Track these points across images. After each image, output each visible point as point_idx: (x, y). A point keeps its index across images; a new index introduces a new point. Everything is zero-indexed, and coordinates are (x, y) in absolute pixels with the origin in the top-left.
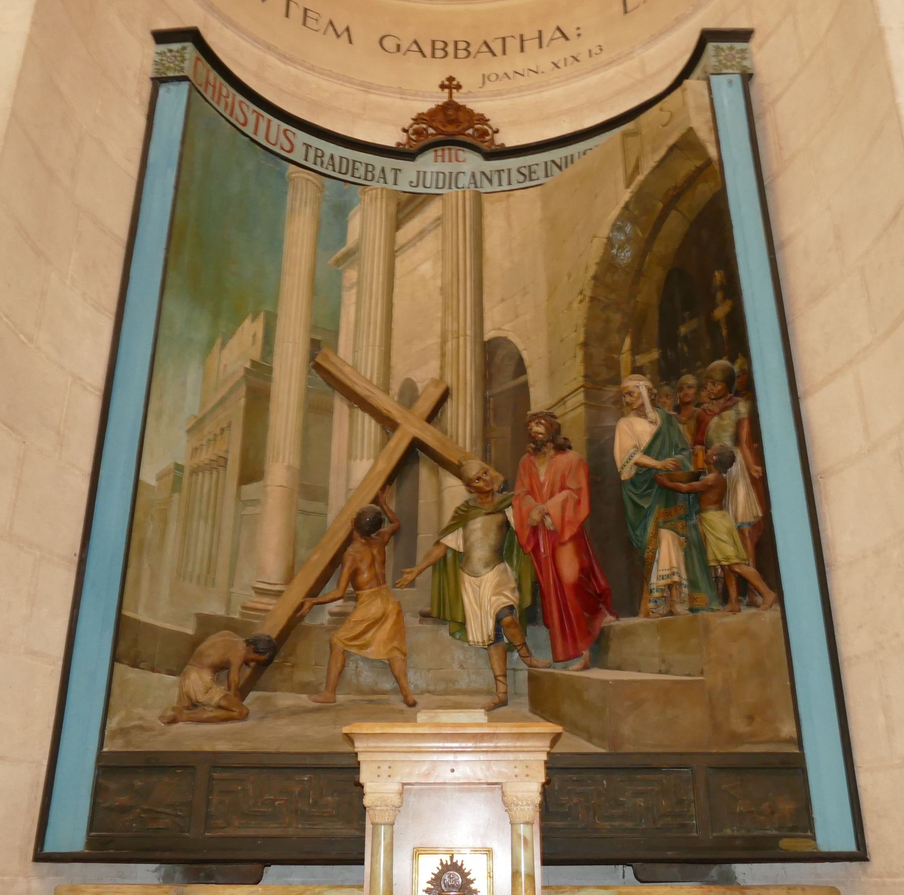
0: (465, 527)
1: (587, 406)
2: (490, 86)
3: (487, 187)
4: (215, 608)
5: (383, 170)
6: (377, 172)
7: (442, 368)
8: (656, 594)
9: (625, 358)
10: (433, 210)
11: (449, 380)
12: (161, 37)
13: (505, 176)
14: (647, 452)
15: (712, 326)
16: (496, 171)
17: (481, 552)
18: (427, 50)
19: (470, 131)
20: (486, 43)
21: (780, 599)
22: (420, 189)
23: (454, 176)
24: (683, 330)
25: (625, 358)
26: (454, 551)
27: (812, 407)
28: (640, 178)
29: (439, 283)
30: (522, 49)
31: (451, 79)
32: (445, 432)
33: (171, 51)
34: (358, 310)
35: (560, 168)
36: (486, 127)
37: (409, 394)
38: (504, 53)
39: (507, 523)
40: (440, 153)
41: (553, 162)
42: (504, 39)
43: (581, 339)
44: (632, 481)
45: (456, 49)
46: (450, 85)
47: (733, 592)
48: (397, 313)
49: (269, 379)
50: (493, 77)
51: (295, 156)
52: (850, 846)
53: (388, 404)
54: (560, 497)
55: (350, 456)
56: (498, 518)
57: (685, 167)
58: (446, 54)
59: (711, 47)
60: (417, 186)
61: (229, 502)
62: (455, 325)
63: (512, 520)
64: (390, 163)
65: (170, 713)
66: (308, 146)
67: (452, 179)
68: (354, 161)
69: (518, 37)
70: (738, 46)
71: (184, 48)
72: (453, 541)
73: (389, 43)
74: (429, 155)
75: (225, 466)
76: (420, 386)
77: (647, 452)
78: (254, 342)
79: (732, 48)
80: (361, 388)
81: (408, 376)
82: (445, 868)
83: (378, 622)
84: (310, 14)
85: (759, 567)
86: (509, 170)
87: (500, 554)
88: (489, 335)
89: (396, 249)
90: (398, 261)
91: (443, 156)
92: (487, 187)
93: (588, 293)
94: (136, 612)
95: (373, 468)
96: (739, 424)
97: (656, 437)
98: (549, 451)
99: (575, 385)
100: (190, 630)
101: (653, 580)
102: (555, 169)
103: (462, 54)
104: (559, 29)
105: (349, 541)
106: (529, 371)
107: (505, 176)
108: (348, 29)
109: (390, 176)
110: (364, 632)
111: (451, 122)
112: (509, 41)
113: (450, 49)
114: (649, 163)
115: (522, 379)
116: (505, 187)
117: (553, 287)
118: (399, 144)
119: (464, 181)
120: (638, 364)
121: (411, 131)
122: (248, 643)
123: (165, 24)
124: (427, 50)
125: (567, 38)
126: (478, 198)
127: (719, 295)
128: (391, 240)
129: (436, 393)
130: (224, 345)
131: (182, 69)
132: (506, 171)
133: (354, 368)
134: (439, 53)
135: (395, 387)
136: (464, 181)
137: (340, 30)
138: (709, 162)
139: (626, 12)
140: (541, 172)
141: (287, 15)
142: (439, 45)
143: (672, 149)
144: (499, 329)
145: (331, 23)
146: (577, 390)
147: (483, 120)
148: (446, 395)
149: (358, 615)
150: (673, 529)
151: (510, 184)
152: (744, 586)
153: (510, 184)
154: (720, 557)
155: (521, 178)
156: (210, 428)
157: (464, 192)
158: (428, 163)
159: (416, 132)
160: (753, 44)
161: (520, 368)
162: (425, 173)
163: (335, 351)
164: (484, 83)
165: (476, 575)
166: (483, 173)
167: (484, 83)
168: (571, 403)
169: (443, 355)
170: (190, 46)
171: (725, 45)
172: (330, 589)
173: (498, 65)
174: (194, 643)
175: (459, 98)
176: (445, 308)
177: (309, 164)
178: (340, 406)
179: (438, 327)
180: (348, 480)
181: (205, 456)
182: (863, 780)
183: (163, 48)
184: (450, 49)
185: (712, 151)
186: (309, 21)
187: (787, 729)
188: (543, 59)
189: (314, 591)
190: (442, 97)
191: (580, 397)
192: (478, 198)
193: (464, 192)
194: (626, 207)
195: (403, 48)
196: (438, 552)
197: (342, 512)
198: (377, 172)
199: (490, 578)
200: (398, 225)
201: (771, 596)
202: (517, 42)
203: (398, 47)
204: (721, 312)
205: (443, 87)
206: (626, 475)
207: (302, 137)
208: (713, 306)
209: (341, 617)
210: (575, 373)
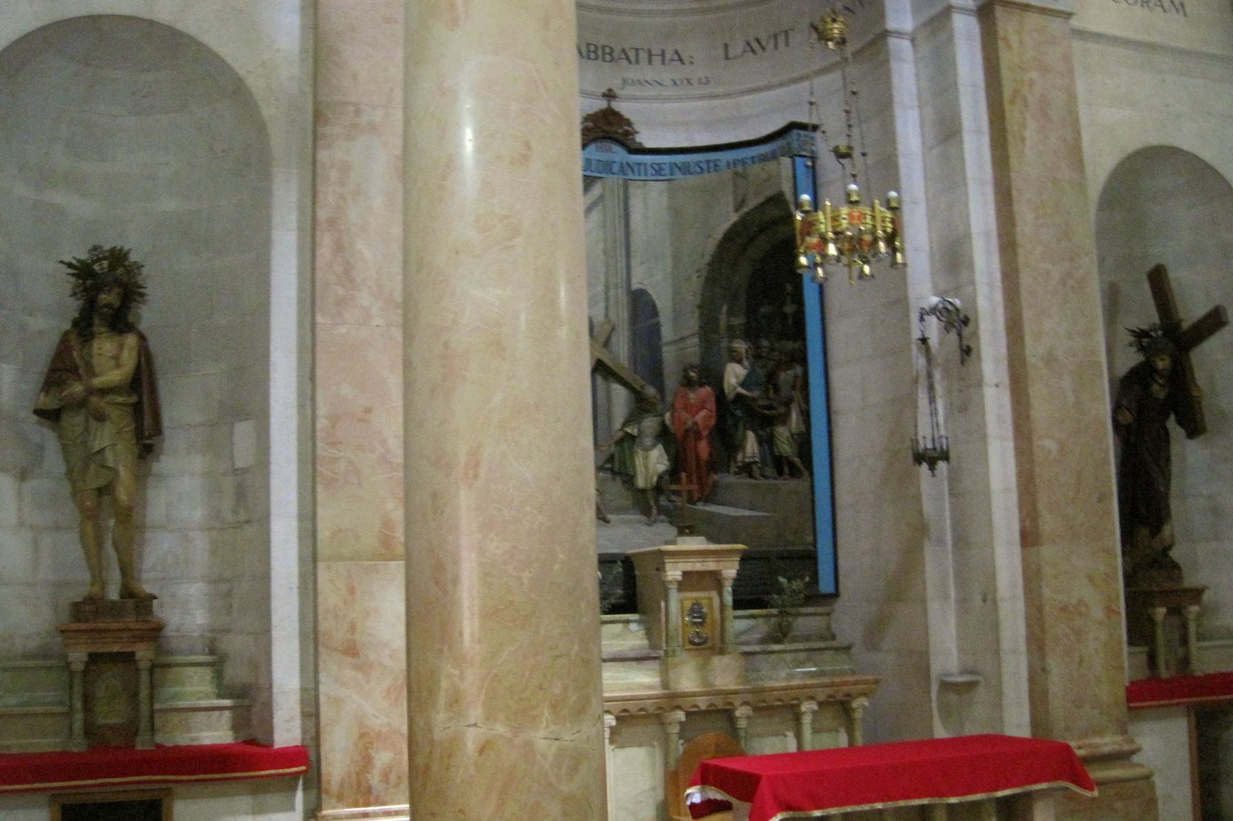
0: (640, 423)
1: (700, 346)
2: (629, 91)
7: (607, 308)
8: (740, 464)
9: (723, 320)
13: (642, 167)
14: (743, 385)
15: (784, 316)
20: (624, 51)
21: (811, 474)
24: (763, 310)
27: (835, 374)
28: (745, 209)
29: (601, 246)
30: (650, 62)
31: (610, 90)
32: (611, 352)
35: (680, 169)
36: (629, 128)
41: (675, 164)
43: (698, 301)
45: (604, 53)
46: (610, 95)
47: (786, 469)
50: (630, 82)
54: (703, 413)
56: (658, 419)
57: (775, 213)
77: (743, 385)
82: (694, 604)
85: (800, 457)
88: (635, 286)
92: (631, 177)
93: (704, 273)
97: (748, 375)
101: (740, 457)
102: (678, 173)
104: (677, 52)
106: (660, 314)
107: (642, 167)
111: (610, 124)
112: (641, 51)
113: (600, 52)
114: (753, 203)
115: (654, 321)
117: (676, 258)
119: (616, 168)
120: (732, 323)
125: (683, 63)
127: (789, 298)
129: (607, 328)
136: (616, 168)
139: (727, 58)
140: (667, 171)
143: (769, 200)
144: (640, 283)
147: (629, 123)
148: (613, 329)
150: (754, 431)
152: (792, 465)
154: (782, 451)
155: (653, 172)
161: (654, 312)
165: (647, 450)
166: (628, 164)
168: (689, 342)
169: (607, 299)
173: (633, 73)
175: (617, 106)
176: (607, 266)
179: (602, 279)
182: (841, 562)
184: (600, 52)
188: (666, 75)
190: (602, 104)
191: (696, 340)
192: (626, 181)
194: (734, 225)
196: (621, 434)
201: (806, 474)
204: (789, 309)
205: (604, 95)
208: (783, 303)
210: (692, 324)
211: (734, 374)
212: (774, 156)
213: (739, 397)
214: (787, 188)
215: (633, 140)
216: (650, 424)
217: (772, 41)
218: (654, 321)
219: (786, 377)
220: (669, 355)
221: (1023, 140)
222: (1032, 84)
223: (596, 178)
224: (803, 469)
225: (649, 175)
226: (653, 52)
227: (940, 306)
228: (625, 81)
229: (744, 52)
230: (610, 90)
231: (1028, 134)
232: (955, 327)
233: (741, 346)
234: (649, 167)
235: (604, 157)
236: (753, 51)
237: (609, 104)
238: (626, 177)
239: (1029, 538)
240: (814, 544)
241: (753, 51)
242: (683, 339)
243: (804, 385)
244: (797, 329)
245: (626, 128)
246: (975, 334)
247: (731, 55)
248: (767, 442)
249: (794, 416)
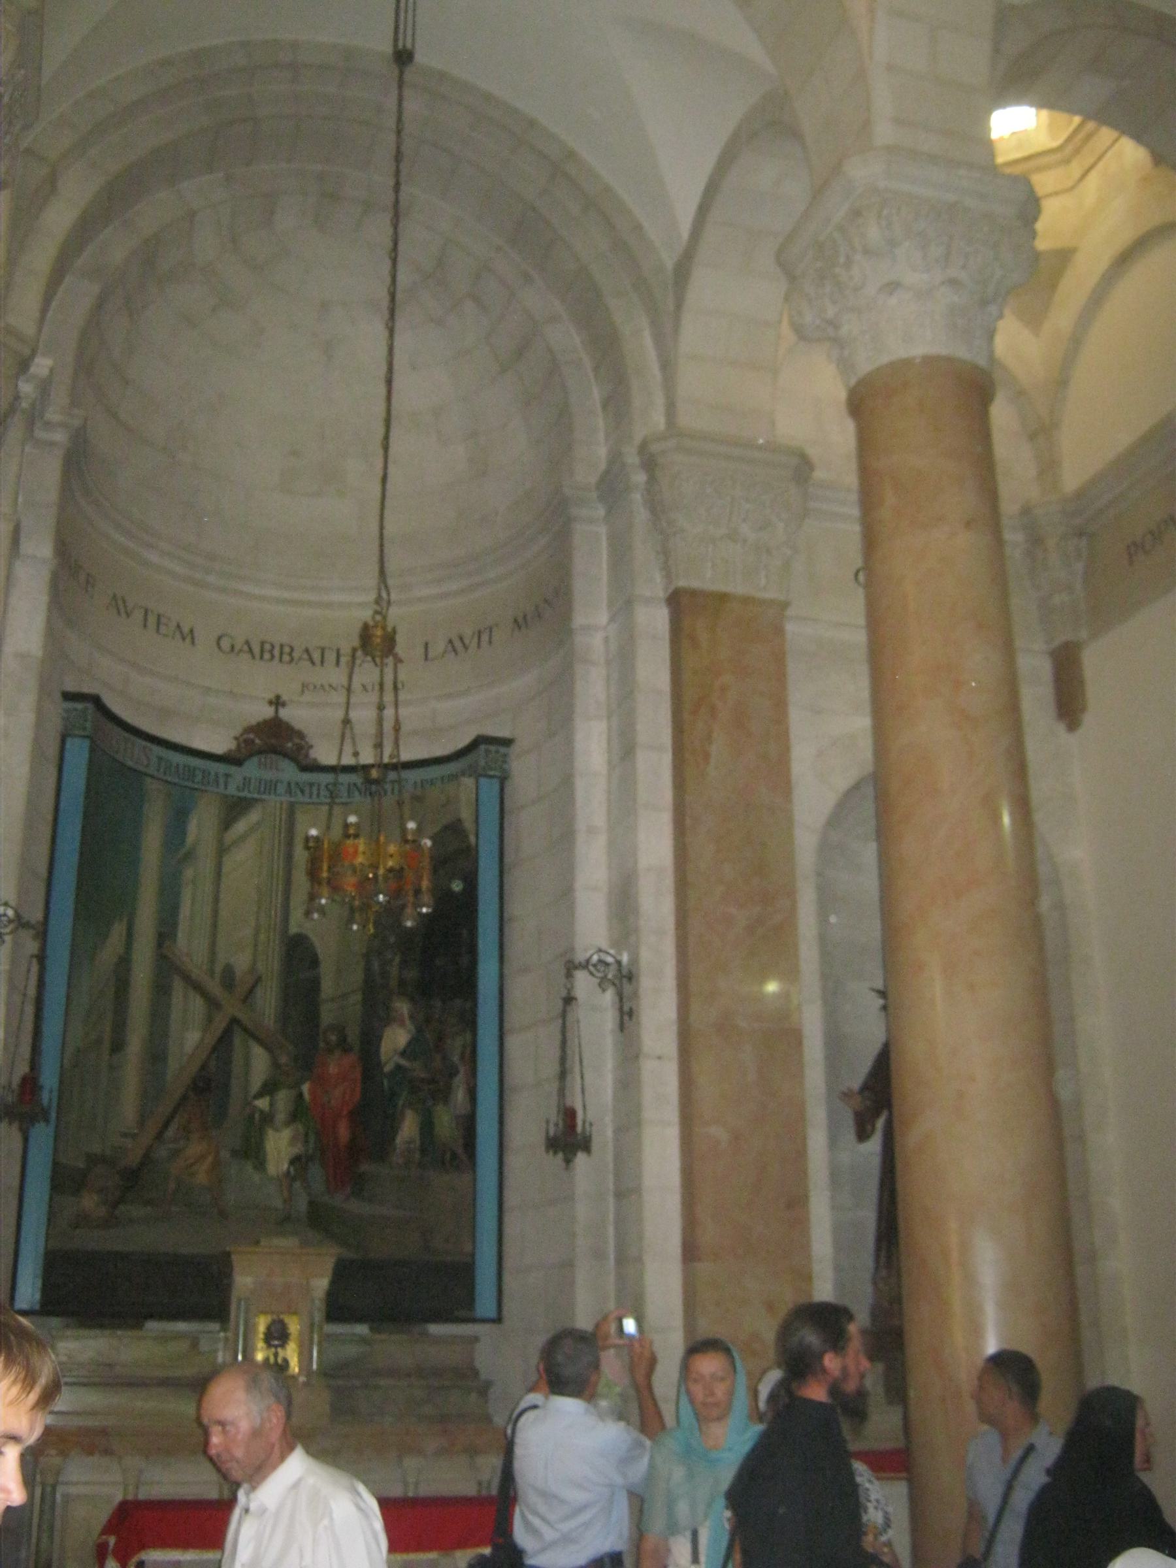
2: (308, 697)
3: (300, 798)
4: (96, 1148)
6: (212, 777)
10: (254, 816)
11: (260, 967)
12: (68, 696)
14: (403, 1054)
17: (281, 1117)
18: (256, 650)
19: (290, 745)
20: (307, 651)
22: (245, 794)
25: (394, 971)
26: (262, 1112)
27: (512, 1042)
31: (278, 697)
33: (76, 710)
34: (193, 904)
35: (360, 794)
37: (228, 978)
38: (322, 662)
39: (301, 1095)
40: (263, 760)
41: (355, 784)
42: (323, 650)
43: (364, 951)
44: (392, 1074)
45: (281, 653)
46: (277, 702)
49: (129, 970)
50: (311, 687)
51: (151, 770)
52: (492, 1314)
53: (214, 987)
58: (273, 657)
59: (483, 747)
60: (243, 790)
63: (307, 1096)
64: (222, 768)
66: (160, 759)
67: (271, 787)
68: (195, 769)
69: (335, 651)
70: (503, 750)
71: (86, 709)
72: (263, 1103)
73: (226, 644)
74: (255, 759)
76: (238, 973)
79: (497, 752)
80: (196, 973)
82: (274, 1322)
83: (203, 1157)
84: (163, 620)
87: (294, 1117)
88: (293, 930)
92: (300, 798)
95: (202, 1039)
96: (464, 1046)
98: (337, 1053)
100: (82, 1166)
102: (357, 793)
103: (286, 658)
108: (191, 631)
110: (192, 1165)
113: (276, 652)
116: (315, 799)
118: (230, 751)
119: (281, 789)
121: (241, 739)
123: (71, 687)
124: (256, 650)
126: (292, 810)
128: (220, 841)
131: (85, 729)
132: (316, 785)
134: (267, 656)
136: (281, 789)
137: (186, 630)
138: (469, 848)
139: (426, 659)
141: (145, 626)
142: (267, 647)
143: (446, 828)
145: (178, 626)
147: (301, 735)
151: (318, 795)
152: (454, 1156)
153: (318, 795)
158: (252, 769)
159: (246, 741)
160: (515, 750)
161: (315, 962)
164: (303, 691)
165: (277, 1130)
166: (297, 784)
167: (303, 691)
170: (90, 706)
171: (493, 748)
172: (170, 1133)
175: (284, 714)
177: (161, 776)
178: (178, 985)
182: (507, 1277)
183: (70, 705)
184: (276, 652)
185: (472, 839)
186: (163, 629)
187: (468, 1248)
189: (159, 1136)
190: (268, 712)
191: (358, 997)
193: (281, 803)
195: (237, 648)
198: (212, 777)
199: (286, 1134)
200: (227, 823)
202: (335, 655)
203: (233, 647)
206: (387, 1069)
207: (157, 750)
209: (175, 1153)
210: (357, 977)
211: (396, 1038)
212: (453, 777)
213: (399, 1067)
214: (466, 815)
215: (307, 756)
216: (283, 1099)
217: (476, 640)
219: (456, 1046)
220: (327, 1016)
221: (707, 756)
222: (723, 689)
223: (256, 800)
224: (464, 1157)
226: (342, 652)
227: (595, 958)
228: (304, 686)
229: (445, 652)
230: (278, 697)
231: (714, 749)
232: (614, 984)
233: (403, 1007)
234: (323, 787)
235: (269, 775)
236: (455, 651)
237: (277, 711)
238: (292, 799)
239: (690, 1252)
240: (473, 1255)
241: (455, 651)
242: (344, 996)
243: (471, 1056)
244: (467, 985)
245: (297, 741)
246: (635, 995)
247: (430, 655)
248: (427, 1127)
249: (460, 1095)
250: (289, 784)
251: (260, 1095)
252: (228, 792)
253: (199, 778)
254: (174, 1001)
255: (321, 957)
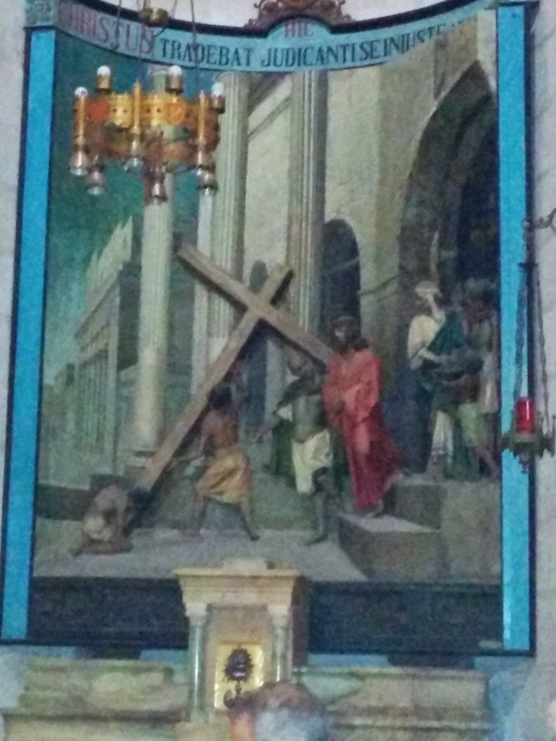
4: (106, 470)
5: (236, 52)
6: (231, 55)
7: (288, 249)
16: (342, 46)
22: (271, 68)
23: (302, 52)
48: (249, 202)
55: (209, 334)
60: (269, 65)
61: (111, 385)
62: (299, 209)
65: (76, 547)
68: (209, 47)
74: (281, 30)
75: (106, 357)
78: (124, 247)
81: (258, 258)
86: (353, 45)
89: (249, 132)
90: (251, 147)
91: (293, 30)
94: (47, 478)
95: (227, 345)
99: (389, 276)
105: (205, 412)
109: (243, 60)
116: (349, 64)
119: (312, 56)
122: (130, 495)
130: (100, 254)
133: (212, 258)
135: (247, 271)
136: (312, 56)
146: (393, 278)
149: (211, 471)
153: (353, 60)
156: (93, 329)
157: (310, 73)
162: (276, 50)
163: (194, 242)
169: (289, 238)
174: (94, 493)
180: (207, 354)
181: (90, 352)
191: (392, 288)
193: (310, 73)
197: (200, 387)
198: (231, 55)
215: (339, 13)
218: (353, 262)
225: (357, 57)
234: (358, 49)
250: (320, 50)
251: (281, 404)
252: (248, 69)
253: (216, 57)
254: (197, 305)
255: (360, 246)
